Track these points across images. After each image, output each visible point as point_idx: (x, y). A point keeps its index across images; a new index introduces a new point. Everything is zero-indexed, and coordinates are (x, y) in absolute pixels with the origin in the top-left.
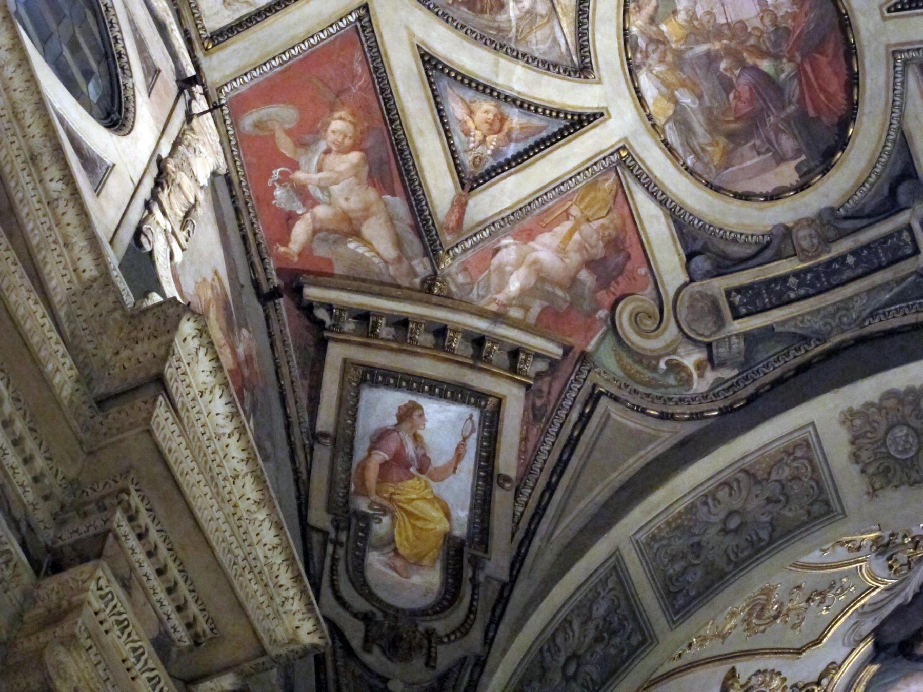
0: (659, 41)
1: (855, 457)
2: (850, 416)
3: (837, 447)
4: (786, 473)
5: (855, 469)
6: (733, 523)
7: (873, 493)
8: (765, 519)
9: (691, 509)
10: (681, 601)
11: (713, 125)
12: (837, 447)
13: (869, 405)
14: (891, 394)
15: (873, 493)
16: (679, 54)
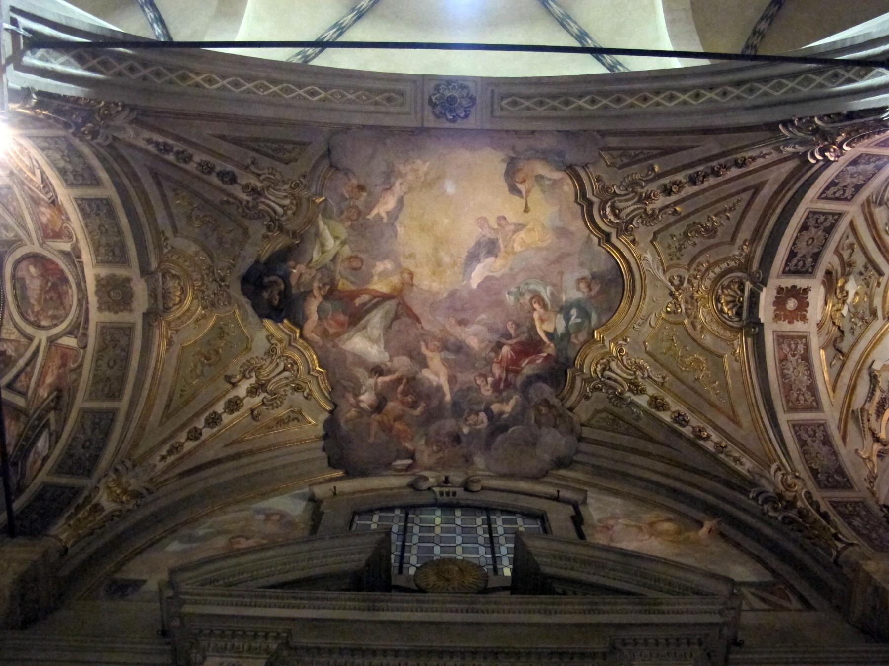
0: (37, 314)
1: (116, 313)
2: (100, 309)
3: (108, 317)
4: (108, 338)
5: (120, 313)
6: (111, 364)
7: (131, 311)
8: (118, 351)
9: (95, 376)
10: (117, 394)
11: (57, 308)
12: (108, 317)
13: (98, 302)
14: (97, 292)
15: (131, 311)
16: (42, 309)
